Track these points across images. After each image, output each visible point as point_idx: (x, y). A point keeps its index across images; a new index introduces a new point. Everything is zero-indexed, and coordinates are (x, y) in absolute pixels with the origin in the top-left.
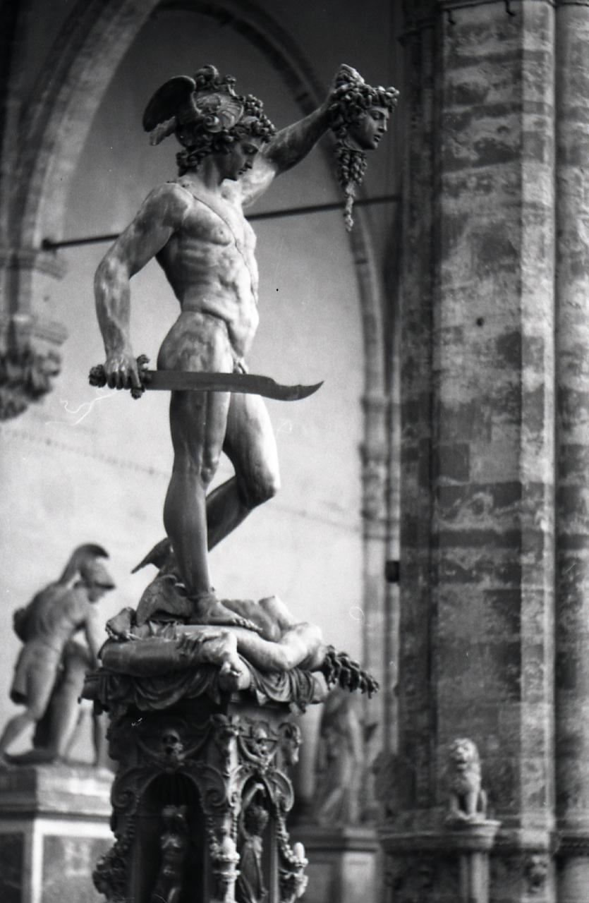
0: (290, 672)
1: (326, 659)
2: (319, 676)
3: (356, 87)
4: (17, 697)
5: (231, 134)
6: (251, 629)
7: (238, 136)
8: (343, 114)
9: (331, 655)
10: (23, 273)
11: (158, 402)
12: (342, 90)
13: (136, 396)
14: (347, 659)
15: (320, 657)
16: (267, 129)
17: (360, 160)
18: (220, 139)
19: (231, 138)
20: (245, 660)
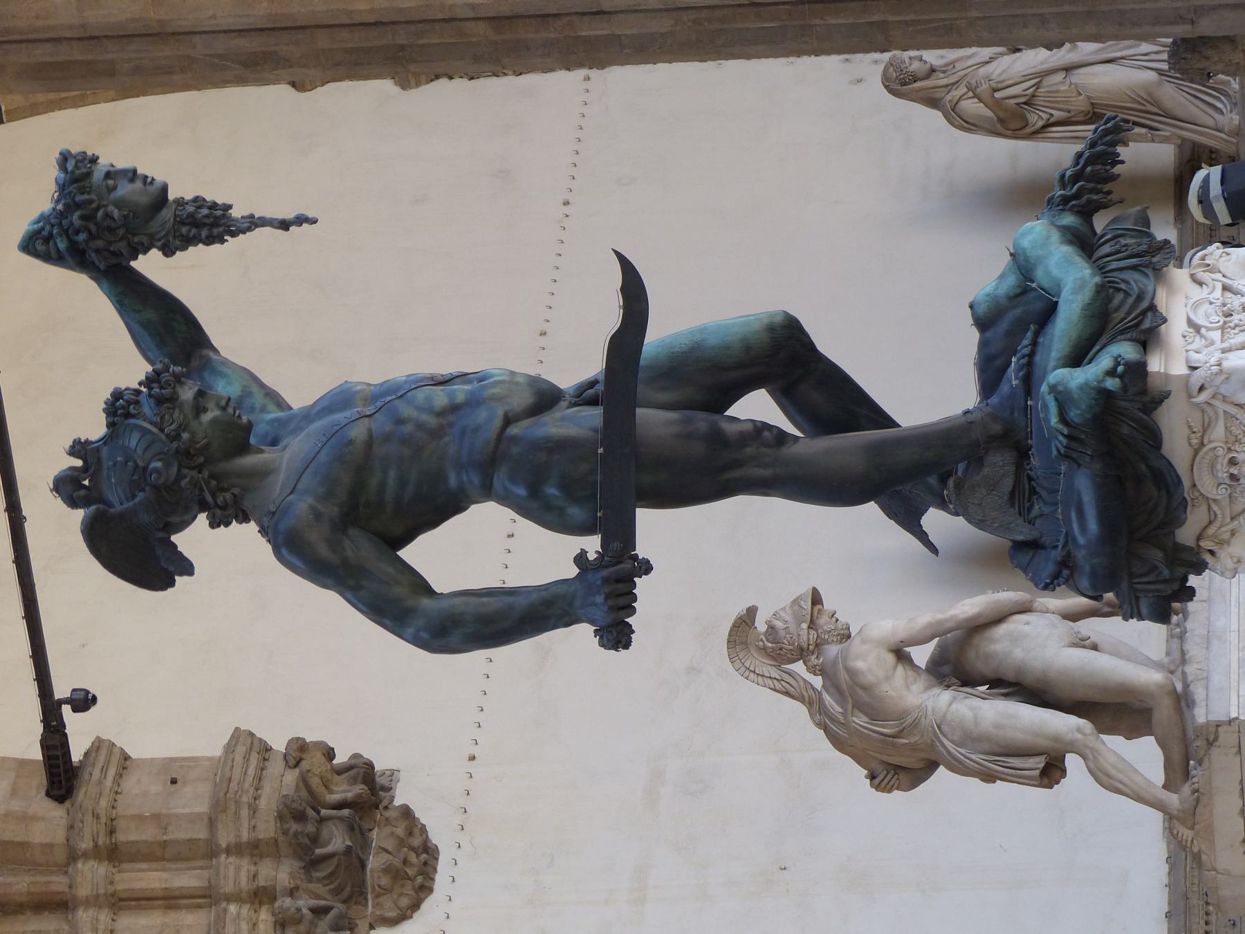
0: (1101, 269)
1: (1071, 209)
2: (1100, 222)
3: (60, 224)
4: (1052, 772)
6: (1034, 343)
7: (180, 425)
8: (110, 243)
9: (1065, 200)
10: (129, 834)
11: (655, 529)
12: (68, 249)
13: (646, 568)
14: (1068, 173)
15: (1069, 219)
19: (185, 436)
20: (1094, 350)
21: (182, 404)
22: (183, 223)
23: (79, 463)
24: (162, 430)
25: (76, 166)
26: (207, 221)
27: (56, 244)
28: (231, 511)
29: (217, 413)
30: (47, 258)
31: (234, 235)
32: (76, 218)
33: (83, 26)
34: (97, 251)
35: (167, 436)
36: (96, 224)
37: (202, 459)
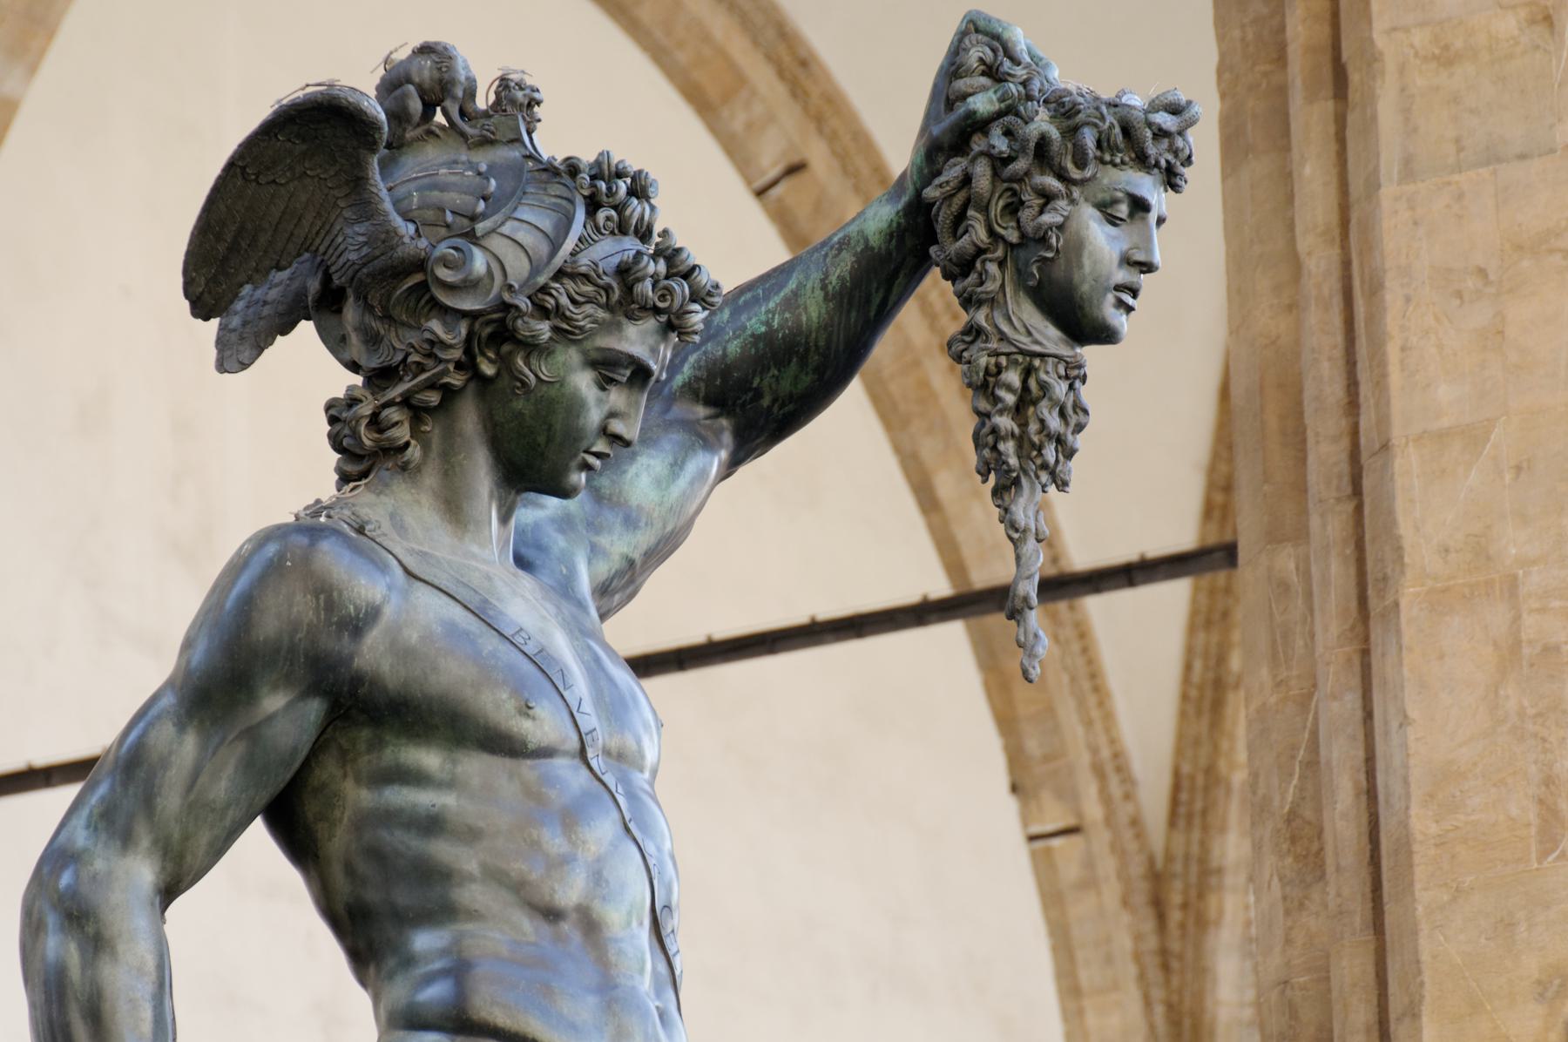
3: (1029, 98)
5: (543, 312)
8: (985, 209)
12: (971, 114)
16: (681, 288)
17: (1060, 389)
18: (498, 330)
19: (544, 329)
21: (619, 326)
22: (1028, 372)
23: (483, 101)
24: (560, 275)
25: (1160, 133)
26: (1033, 427)
27: (984, 89)
28: (367, 439)
29: (594, 417)
30: (953, 69)
31: (997, 492)
32: (1042, 123)
33: (1386, 447)
34: (967, 180)
35: (544, 289)
36: (1027, 173)
37: (488, 369)
